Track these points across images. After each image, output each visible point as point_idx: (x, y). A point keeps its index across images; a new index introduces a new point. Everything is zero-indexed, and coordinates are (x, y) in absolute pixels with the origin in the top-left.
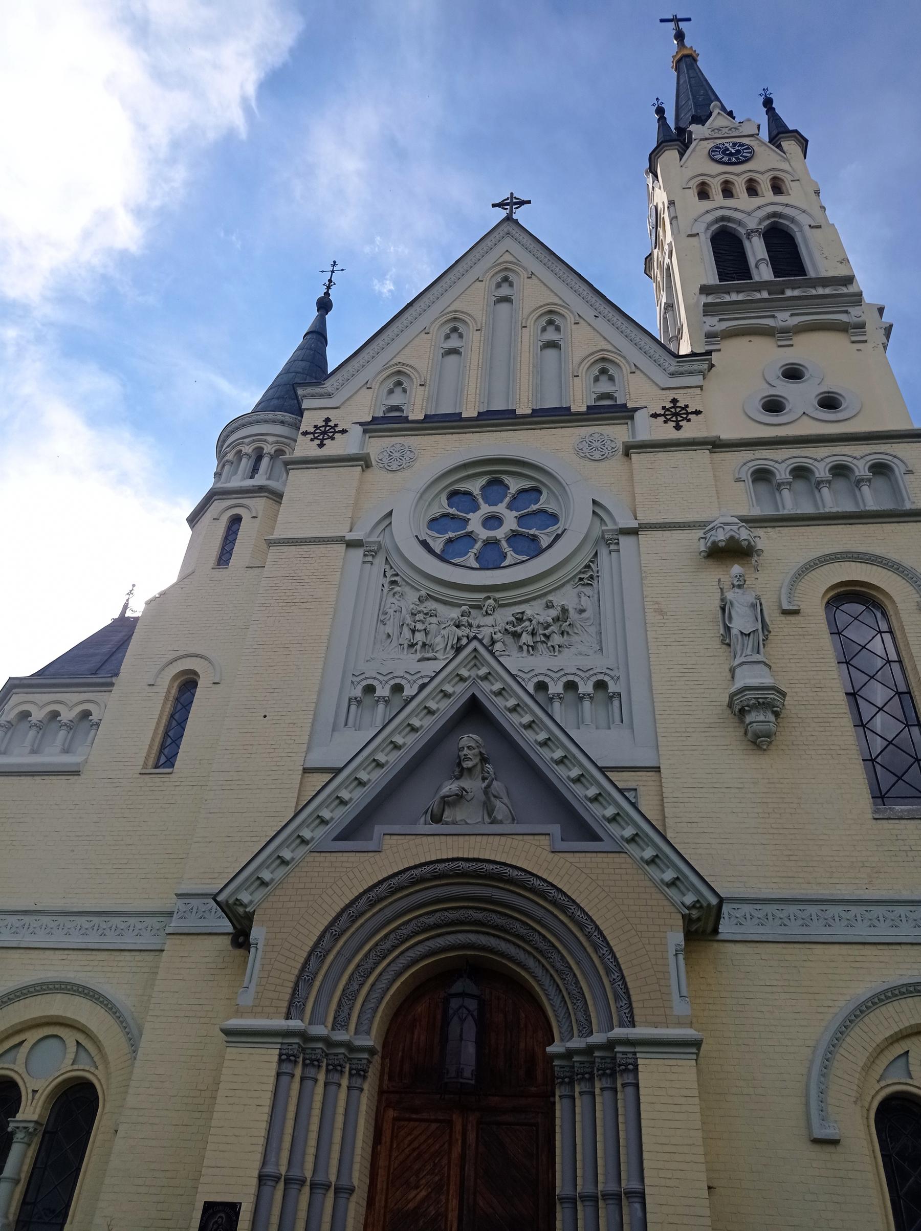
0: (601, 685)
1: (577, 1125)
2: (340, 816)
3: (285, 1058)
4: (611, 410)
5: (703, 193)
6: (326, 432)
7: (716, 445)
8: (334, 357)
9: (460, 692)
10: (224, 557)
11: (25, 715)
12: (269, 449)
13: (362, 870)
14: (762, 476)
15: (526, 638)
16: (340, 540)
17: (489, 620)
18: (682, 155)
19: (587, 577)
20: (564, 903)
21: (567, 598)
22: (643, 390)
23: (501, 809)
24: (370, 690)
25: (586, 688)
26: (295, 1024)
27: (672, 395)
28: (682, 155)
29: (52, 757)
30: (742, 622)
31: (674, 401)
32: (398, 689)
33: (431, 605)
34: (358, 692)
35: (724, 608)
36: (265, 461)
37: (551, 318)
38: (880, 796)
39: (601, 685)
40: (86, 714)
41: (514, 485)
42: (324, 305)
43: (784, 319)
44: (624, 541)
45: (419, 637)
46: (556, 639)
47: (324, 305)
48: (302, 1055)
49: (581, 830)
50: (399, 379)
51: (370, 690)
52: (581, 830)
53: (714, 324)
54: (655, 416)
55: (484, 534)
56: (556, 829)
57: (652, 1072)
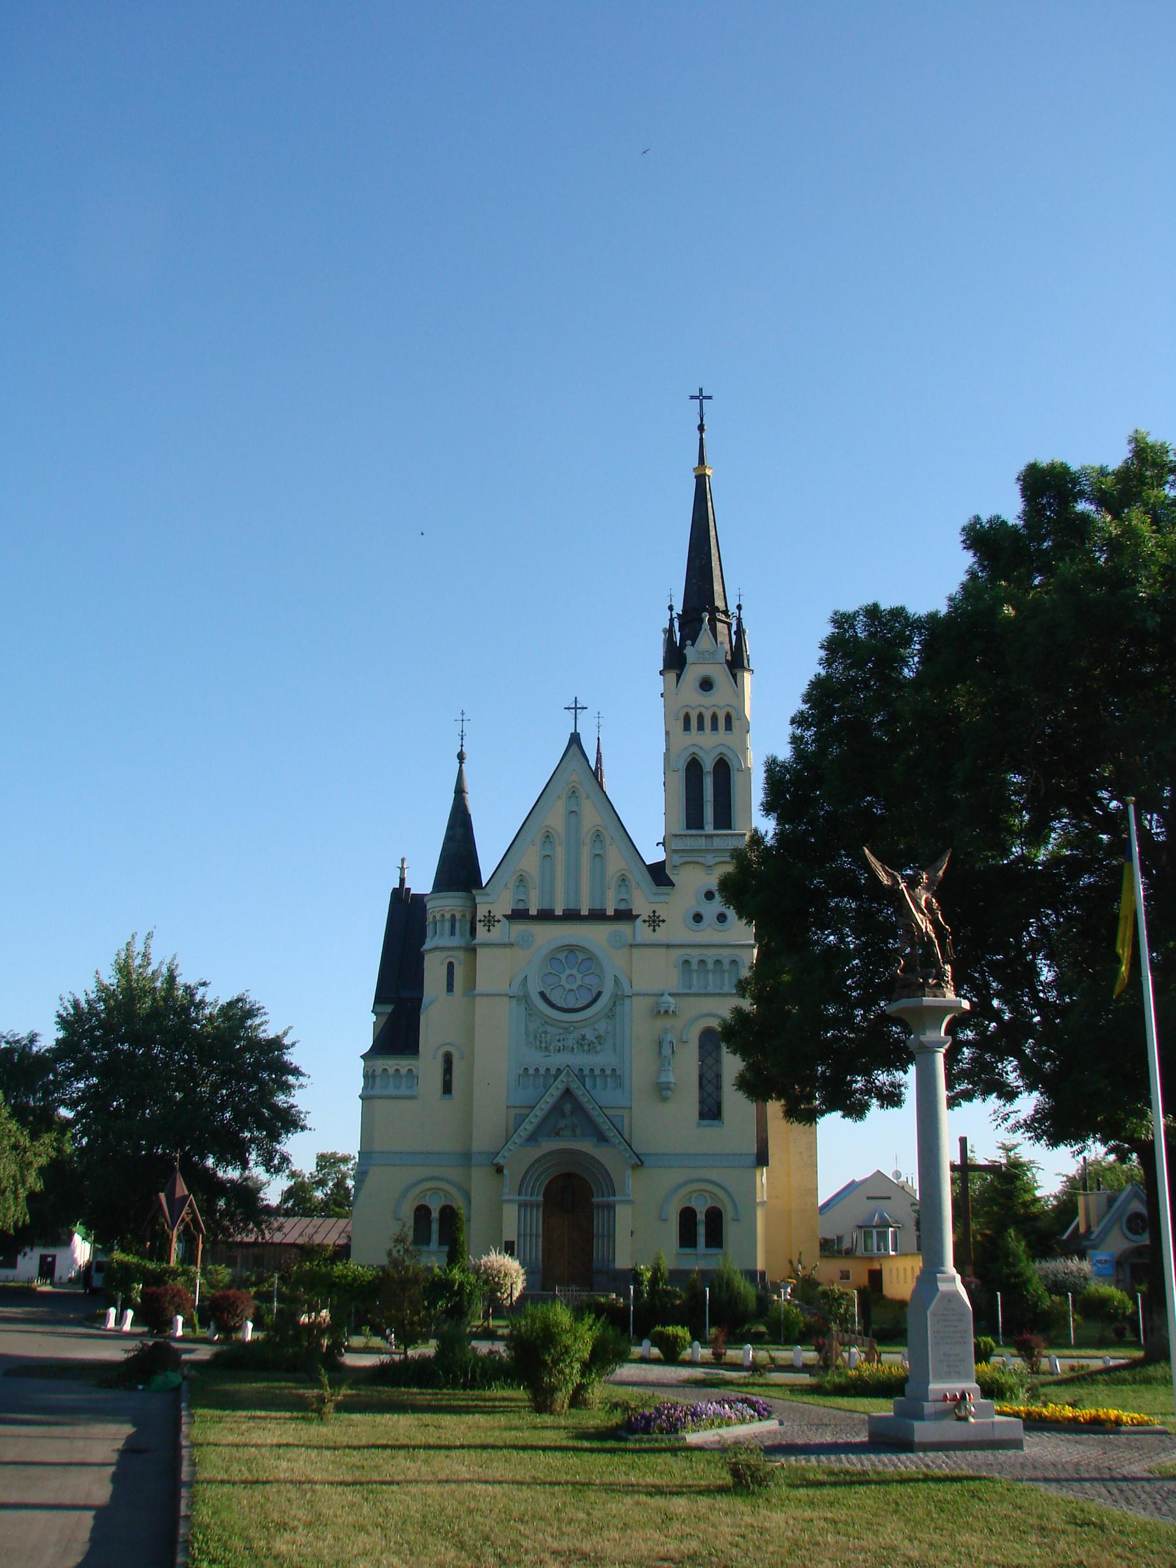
0: (614, 1070)
1: (599, 1218)
2: (524, 1134)
3: (520, 1206)
4: (625, 916)
5: (687, 727)
6: (490, 921)
7: (668, 946)
8: (487, 867)
9: (562, 1087)
10: (450, 987)
11: (385, 1070)
12: (458, 916)
13: (534, 1153)
14: (686, 962)
15: (586, 1048)
16: (506, 995)
17: (571, 1036)
18: (679, 677)
19: (610, 1014)
20: (599, 1162)
21: (602, 1026)
22: (641, 905)
23: (578, 1131)
24: (526, 1069)
25: (608, 1072)
26: (522, 1198)
27: (654, 907)
28: (679, 677)
29: (403, 1091)
30: (667, 1051)
31: (654, 912)
32: (537, 1070)
33: (549, 1029)
34: (521, 1072)
35: (660, 1043)
36: (457, 925)
37: (598, 835)
38: (702, 1116)
39: (614, 1070)
40: (410, 1070)
41: (581, 957)
42: (461, 757)
43: (710, 859)
44: (626, 1000)
45: (543, 1045)
46: (598, 1048)
47: (461, 757)
48: (523, 1205)
49: (602, 1138)
50: (522, 880)
51: (526, 1069)
52: (602, 1138)
53: (677, 859)
54: (645, 921)
55: (568, 987)
56: (595, 1139)
57: (618, 1208)
